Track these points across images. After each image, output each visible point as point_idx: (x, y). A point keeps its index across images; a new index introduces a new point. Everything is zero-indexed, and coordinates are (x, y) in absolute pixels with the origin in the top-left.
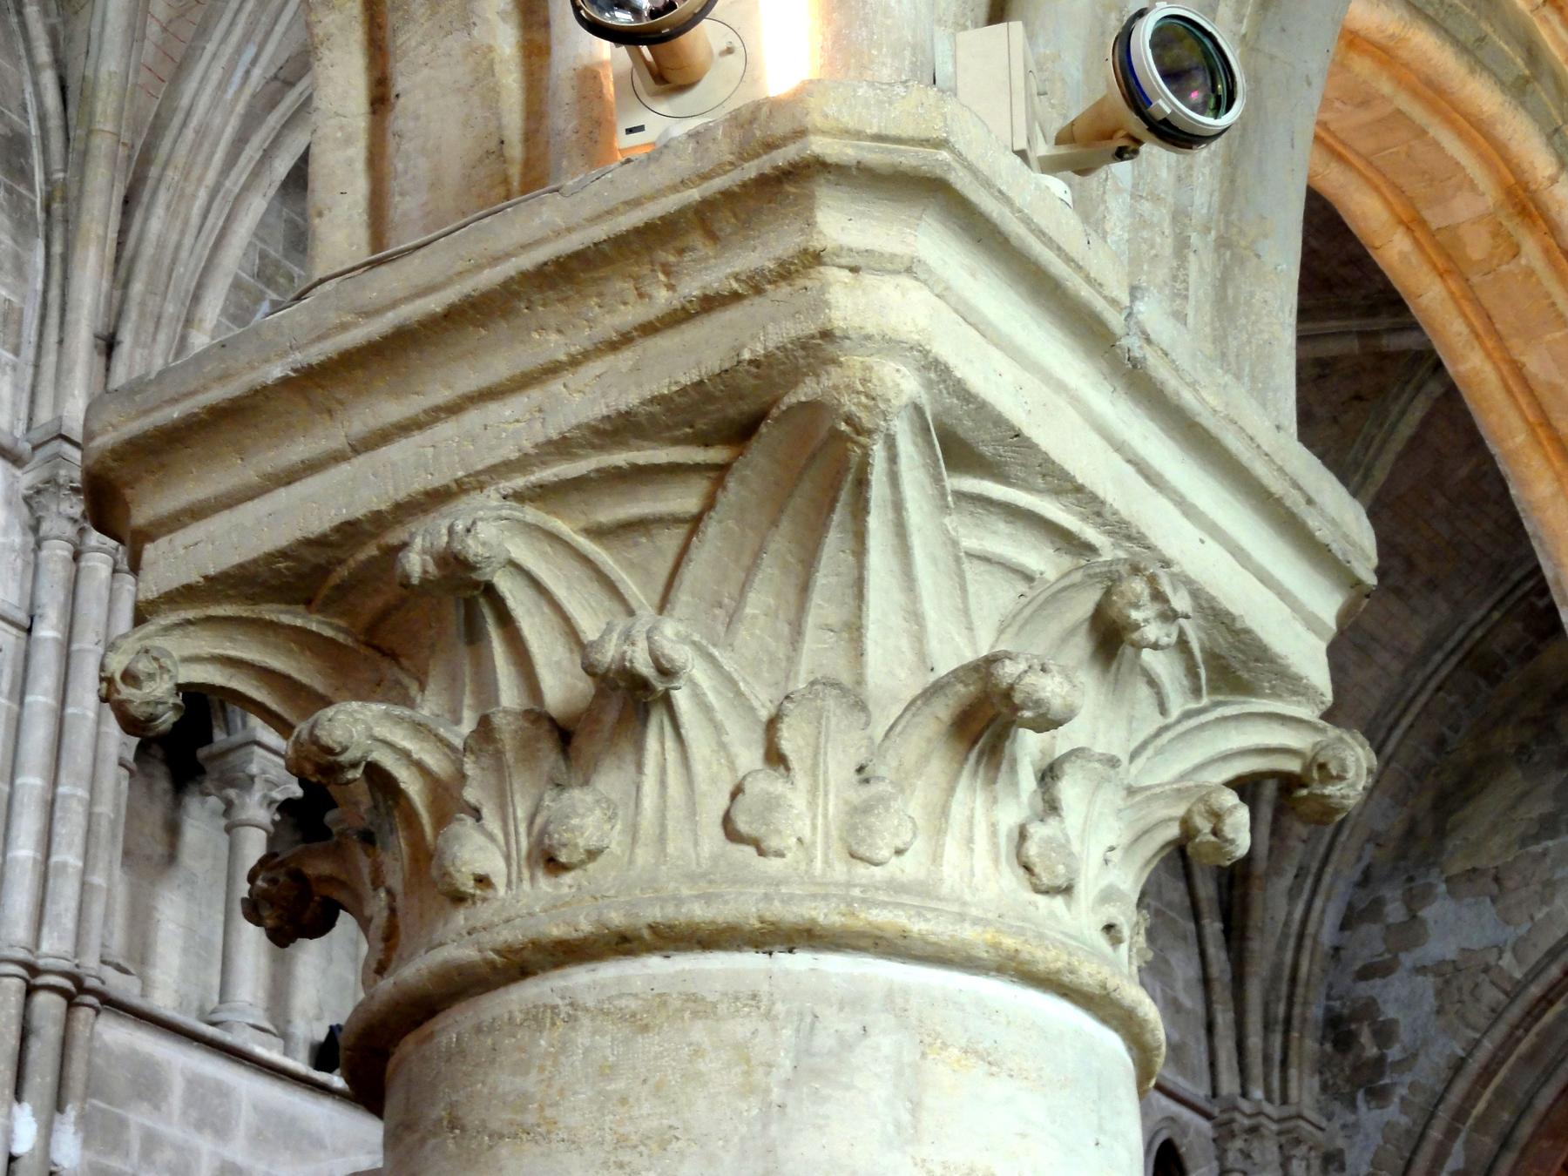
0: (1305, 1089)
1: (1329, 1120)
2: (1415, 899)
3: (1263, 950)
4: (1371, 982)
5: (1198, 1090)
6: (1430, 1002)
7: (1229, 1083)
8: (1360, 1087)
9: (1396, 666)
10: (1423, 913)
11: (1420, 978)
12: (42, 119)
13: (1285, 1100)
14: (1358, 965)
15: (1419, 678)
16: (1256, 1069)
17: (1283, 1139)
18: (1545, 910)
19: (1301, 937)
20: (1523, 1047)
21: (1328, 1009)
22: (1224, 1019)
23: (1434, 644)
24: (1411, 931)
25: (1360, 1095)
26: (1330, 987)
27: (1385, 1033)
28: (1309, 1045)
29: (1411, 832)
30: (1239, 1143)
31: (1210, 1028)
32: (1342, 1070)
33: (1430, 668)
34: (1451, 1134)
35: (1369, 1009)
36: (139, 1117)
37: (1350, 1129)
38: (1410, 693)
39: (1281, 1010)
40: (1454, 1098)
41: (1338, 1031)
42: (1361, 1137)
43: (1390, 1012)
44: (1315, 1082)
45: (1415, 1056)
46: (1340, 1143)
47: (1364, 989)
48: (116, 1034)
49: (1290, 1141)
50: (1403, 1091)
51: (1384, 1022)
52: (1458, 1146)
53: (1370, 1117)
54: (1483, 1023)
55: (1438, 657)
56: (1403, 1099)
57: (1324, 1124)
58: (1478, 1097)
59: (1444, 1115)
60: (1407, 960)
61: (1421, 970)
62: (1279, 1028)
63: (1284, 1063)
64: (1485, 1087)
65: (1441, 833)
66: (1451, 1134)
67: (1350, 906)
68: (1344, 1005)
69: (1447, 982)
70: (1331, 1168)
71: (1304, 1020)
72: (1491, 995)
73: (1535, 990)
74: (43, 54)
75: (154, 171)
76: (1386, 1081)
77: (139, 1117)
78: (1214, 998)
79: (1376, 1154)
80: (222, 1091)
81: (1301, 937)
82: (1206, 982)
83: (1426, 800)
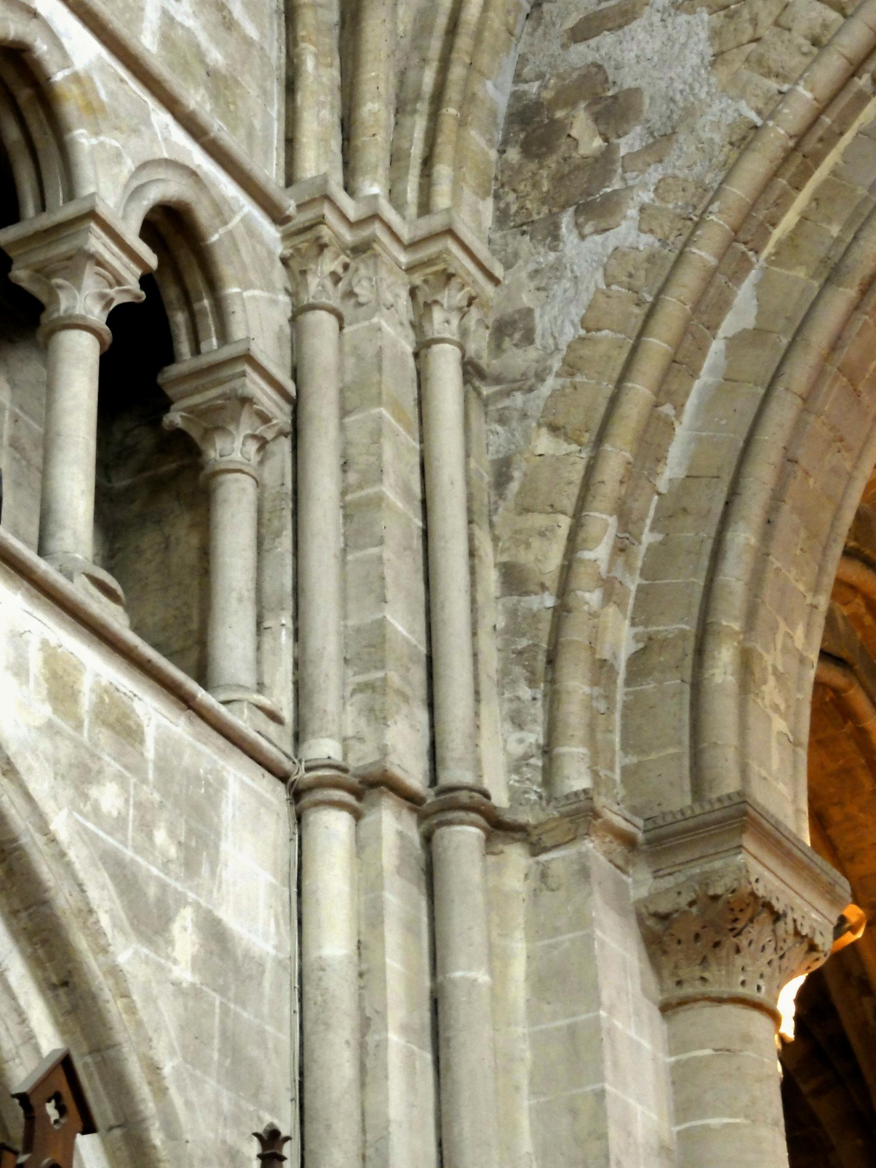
1: (508, 266)
4: (593, 42)
8: (564, 207)
13: (425, 207)
14: (571, 22)
17: (417, 279)
21: (516, 96)
25: (566, 219)
26: (523, 60)
30: (329, 264)
32: (536, 185)
39: (429, 78)
42: (566, 284)
44: (488, 207)
46: (526, 299)
50: (646, 197)
51: (615, 97)
56: (642, 209)
57: (498, 271)
58: (782, 203)
62: (423, 107)
63: (428, 163)
64: (798, 188)
68: (545, 87)
70: (507, 343)
71: (469, 99)
78: (302, 33)
79: (590, 307)
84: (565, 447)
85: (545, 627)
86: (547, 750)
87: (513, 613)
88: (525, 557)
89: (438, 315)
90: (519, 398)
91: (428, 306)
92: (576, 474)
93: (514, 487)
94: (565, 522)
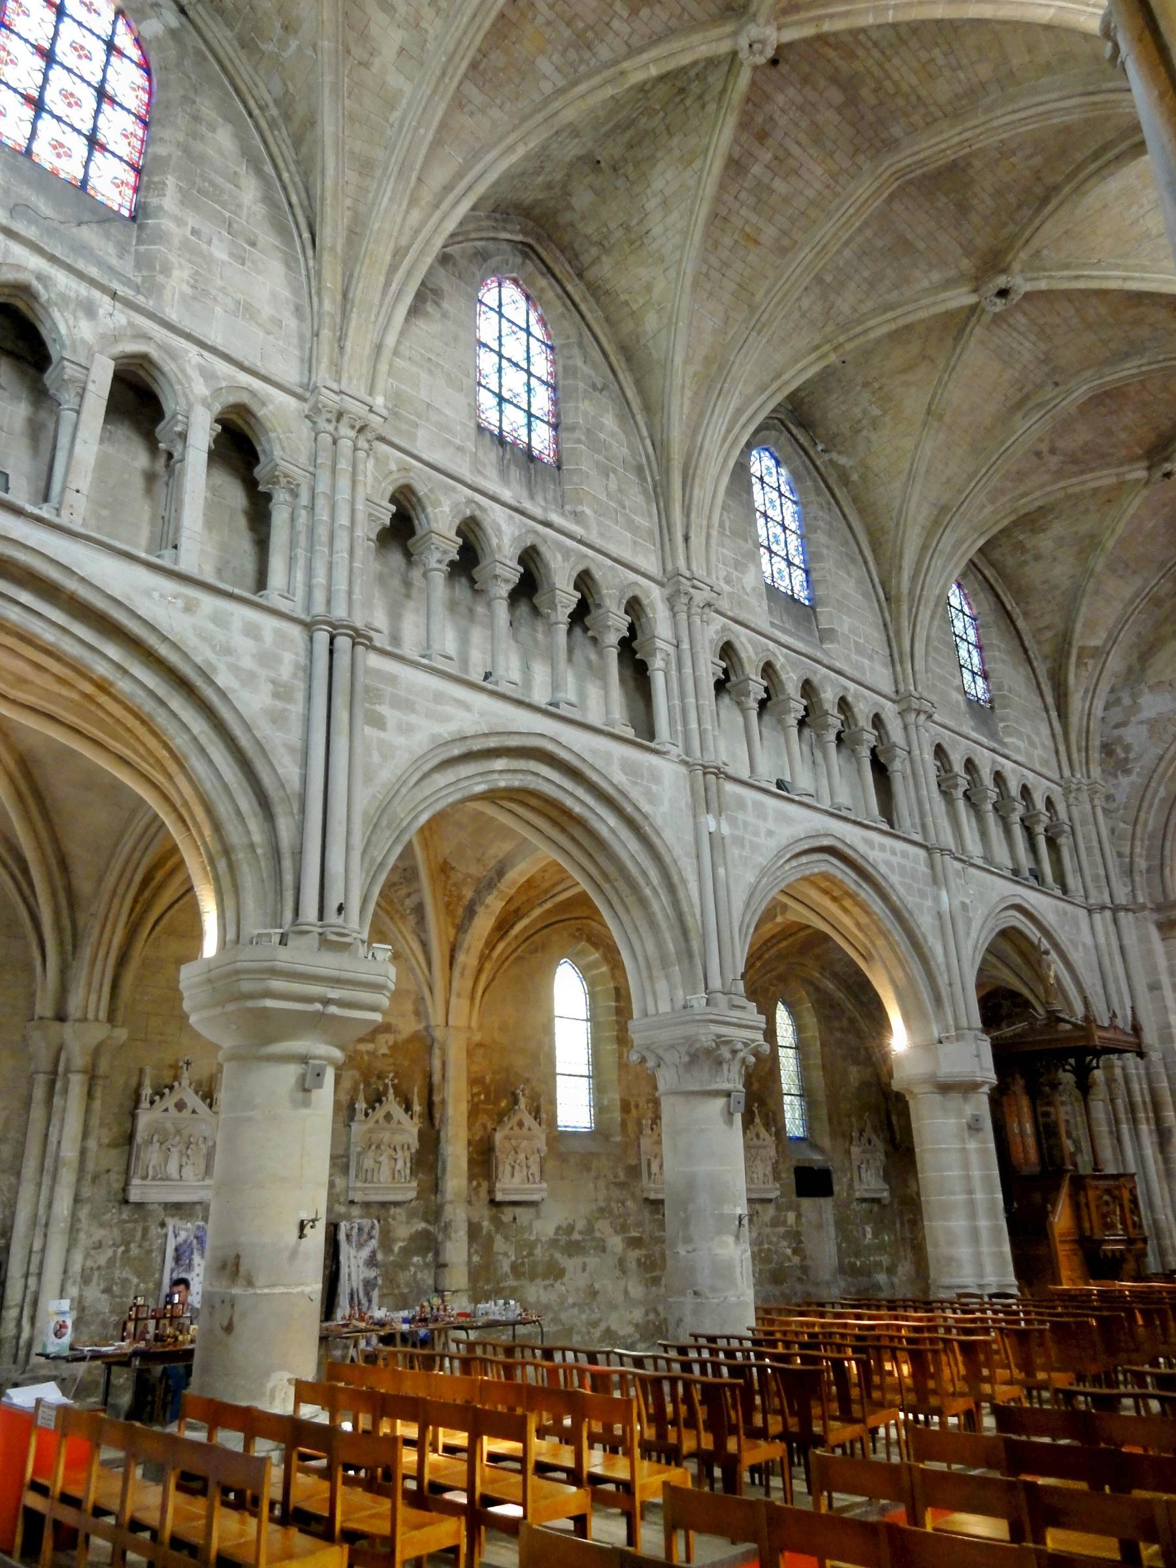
0: (1096, 771)
2: (1134, 696)
3: (1075, 720)
5: (1056, 777)
7: (1067, 772)
12: (648, 457)
16: (1077, 766)
19: (1089, 714)
22: (1062, 748)
23: (1137, 595)
24: (1135, 708)
27: (1127, 749)
28: (1095, 755)
29: (1130, 670)
31: (1057, 752)
34: (1159, 785)
35: (1120, 739)
36: (741, 816)
37: (1116, 786)
40: (1160, 770)
41: (1107, 749)
43: (1129, 740)
46: (1113, 791)
47: (1116, 732)
48: (729, 787)
49: (1093, 793)
53: (1124, 780)
59: (1156, 776)
61: (1141, 722)
65: (1143, 669)
74: (645, 433)
75: (691, 471)
77: (741, 816)
80: (762, 805)
81: (1089, 714)
82: (1053, 735)
83: (1135, 655)
86: (1133, 891)
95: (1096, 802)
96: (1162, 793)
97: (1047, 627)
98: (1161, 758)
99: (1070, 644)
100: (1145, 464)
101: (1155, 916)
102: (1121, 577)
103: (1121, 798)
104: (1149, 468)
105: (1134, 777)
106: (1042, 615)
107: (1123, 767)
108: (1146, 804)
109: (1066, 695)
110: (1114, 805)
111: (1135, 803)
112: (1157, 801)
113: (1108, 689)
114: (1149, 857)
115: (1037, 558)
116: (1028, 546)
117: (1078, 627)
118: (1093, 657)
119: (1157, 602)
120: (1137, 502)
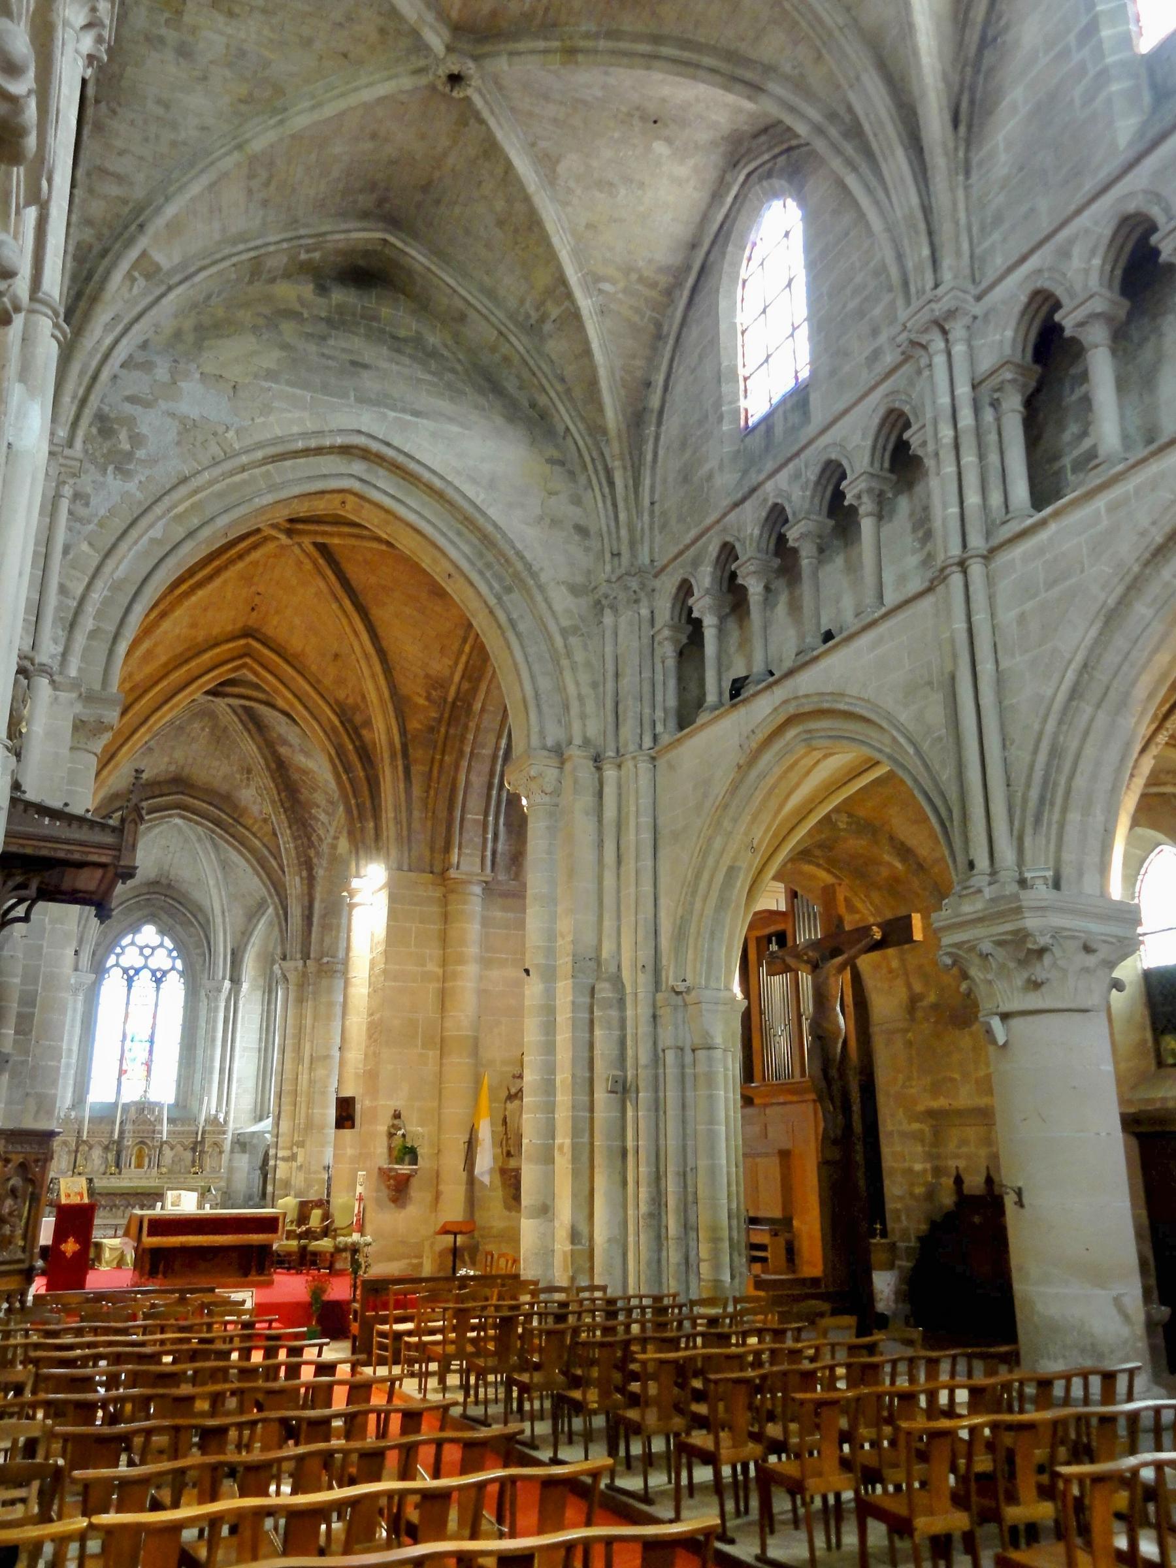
6: (172, 435)
9: (217, 236)
10: (182, 384)
11: (169, 420)
14: (127, 393)
15: (226, 252)
18: (262, 419)
20: (217, 487)
21: (100, 409)
23: (242, 238)
25: (111, 468)
27: (137, 440)
29: (178, 335)
33: (235, 250)
35: (130, 422)
37: (99, 486)
38: (218, 256)
40: (176, 495)
41: (105, 426)
43: (144, 429)
45: (156, 462)
46: (89, 490)
47: (128, 408)
52: (160, 524)
53: (114, 483)
54: (206, 463)
55: (241, 247)
59: (166, 502)
60: (163, 405)
61: (173, 415)
65: (199, 345)
66: (164, 515)
67: (131, 356)
69: (188, 431)
72: (214, 449)
73: (244, 459)
76: (131, 467)
84: (92, 552)
85: (72, 611)
87: (61, 602)
88: (69, 584)
89: (67, 487)
90: (78, 525)
91: (64, 483)
92: (95, 563)
93: (70, 557)
94: (87, 580)
95: (67, 491)
96: (157, 532)
97: (120, 179)
98: (184, 480)
99: (141, 227)
100: (446, 34)
101: (78, 708)
102: (250, 192)
103: (100, 505)
104: (449, 49)
105: (132, 486)
106: (121, 153)
107: (121, 463)
108: (134, 533)
109: (94, 299)
110: (82, 511)
111: (119, 524)
112: (145, 539)
113: (140, 339)
114: (99, 615)
115: (184, 52)
116: (187, 19)
117: (170, 211)
118: (148, 277)
119: (256, 269)
120: (384, 89)
